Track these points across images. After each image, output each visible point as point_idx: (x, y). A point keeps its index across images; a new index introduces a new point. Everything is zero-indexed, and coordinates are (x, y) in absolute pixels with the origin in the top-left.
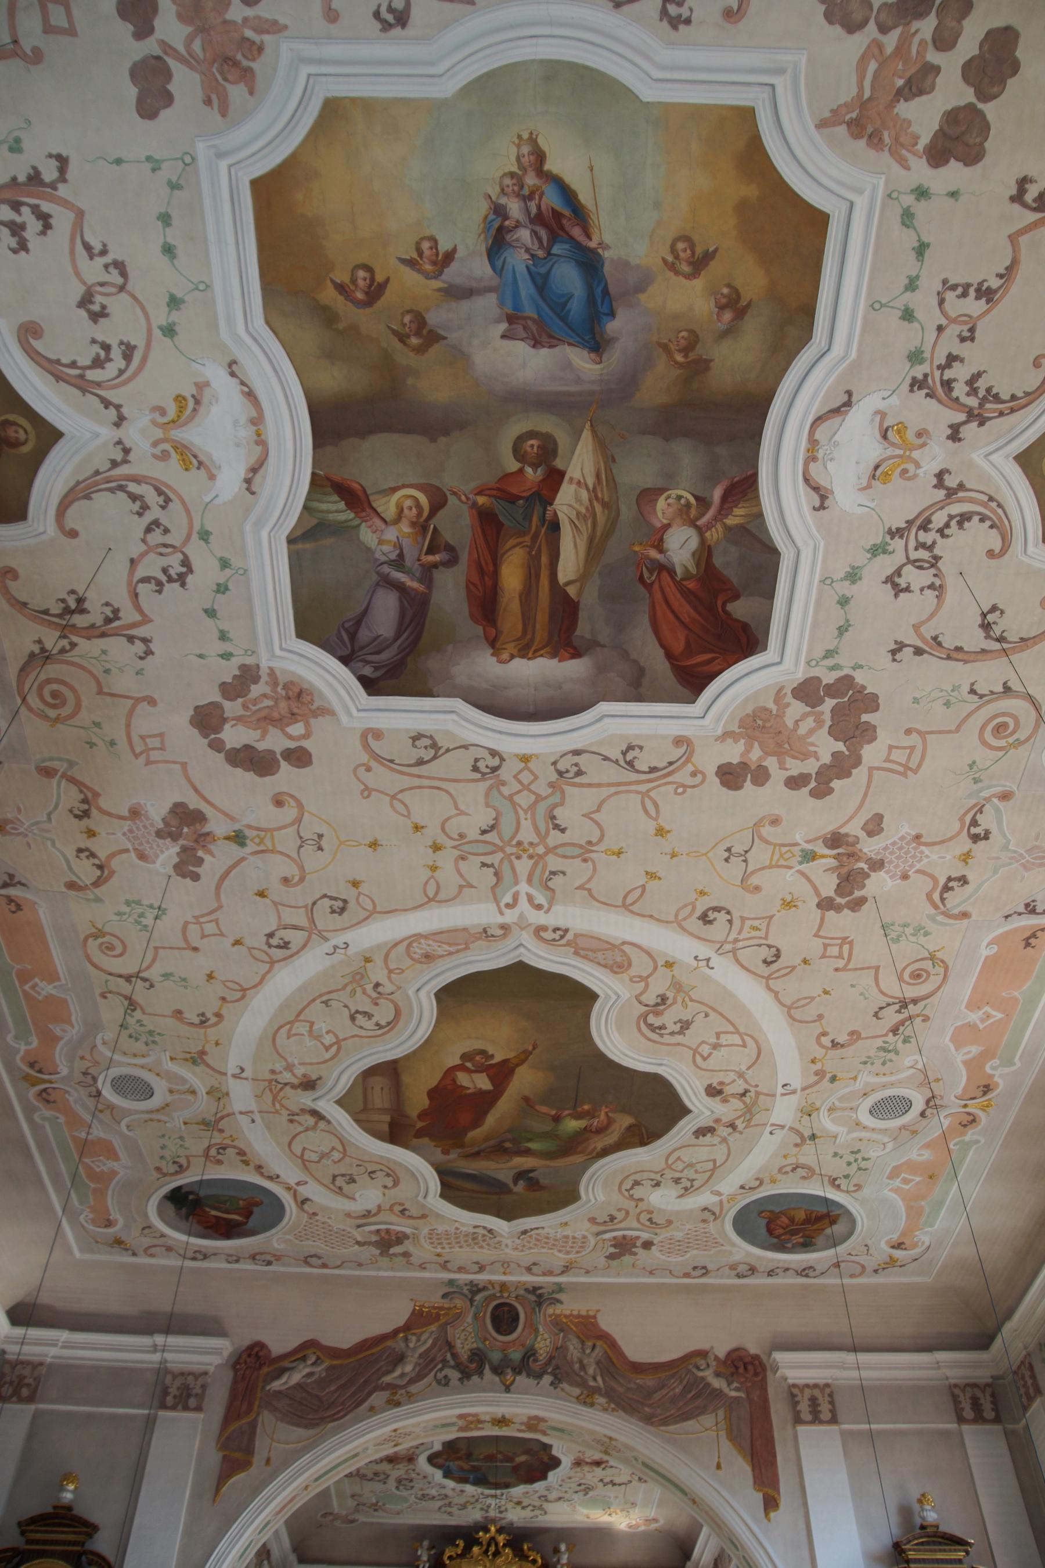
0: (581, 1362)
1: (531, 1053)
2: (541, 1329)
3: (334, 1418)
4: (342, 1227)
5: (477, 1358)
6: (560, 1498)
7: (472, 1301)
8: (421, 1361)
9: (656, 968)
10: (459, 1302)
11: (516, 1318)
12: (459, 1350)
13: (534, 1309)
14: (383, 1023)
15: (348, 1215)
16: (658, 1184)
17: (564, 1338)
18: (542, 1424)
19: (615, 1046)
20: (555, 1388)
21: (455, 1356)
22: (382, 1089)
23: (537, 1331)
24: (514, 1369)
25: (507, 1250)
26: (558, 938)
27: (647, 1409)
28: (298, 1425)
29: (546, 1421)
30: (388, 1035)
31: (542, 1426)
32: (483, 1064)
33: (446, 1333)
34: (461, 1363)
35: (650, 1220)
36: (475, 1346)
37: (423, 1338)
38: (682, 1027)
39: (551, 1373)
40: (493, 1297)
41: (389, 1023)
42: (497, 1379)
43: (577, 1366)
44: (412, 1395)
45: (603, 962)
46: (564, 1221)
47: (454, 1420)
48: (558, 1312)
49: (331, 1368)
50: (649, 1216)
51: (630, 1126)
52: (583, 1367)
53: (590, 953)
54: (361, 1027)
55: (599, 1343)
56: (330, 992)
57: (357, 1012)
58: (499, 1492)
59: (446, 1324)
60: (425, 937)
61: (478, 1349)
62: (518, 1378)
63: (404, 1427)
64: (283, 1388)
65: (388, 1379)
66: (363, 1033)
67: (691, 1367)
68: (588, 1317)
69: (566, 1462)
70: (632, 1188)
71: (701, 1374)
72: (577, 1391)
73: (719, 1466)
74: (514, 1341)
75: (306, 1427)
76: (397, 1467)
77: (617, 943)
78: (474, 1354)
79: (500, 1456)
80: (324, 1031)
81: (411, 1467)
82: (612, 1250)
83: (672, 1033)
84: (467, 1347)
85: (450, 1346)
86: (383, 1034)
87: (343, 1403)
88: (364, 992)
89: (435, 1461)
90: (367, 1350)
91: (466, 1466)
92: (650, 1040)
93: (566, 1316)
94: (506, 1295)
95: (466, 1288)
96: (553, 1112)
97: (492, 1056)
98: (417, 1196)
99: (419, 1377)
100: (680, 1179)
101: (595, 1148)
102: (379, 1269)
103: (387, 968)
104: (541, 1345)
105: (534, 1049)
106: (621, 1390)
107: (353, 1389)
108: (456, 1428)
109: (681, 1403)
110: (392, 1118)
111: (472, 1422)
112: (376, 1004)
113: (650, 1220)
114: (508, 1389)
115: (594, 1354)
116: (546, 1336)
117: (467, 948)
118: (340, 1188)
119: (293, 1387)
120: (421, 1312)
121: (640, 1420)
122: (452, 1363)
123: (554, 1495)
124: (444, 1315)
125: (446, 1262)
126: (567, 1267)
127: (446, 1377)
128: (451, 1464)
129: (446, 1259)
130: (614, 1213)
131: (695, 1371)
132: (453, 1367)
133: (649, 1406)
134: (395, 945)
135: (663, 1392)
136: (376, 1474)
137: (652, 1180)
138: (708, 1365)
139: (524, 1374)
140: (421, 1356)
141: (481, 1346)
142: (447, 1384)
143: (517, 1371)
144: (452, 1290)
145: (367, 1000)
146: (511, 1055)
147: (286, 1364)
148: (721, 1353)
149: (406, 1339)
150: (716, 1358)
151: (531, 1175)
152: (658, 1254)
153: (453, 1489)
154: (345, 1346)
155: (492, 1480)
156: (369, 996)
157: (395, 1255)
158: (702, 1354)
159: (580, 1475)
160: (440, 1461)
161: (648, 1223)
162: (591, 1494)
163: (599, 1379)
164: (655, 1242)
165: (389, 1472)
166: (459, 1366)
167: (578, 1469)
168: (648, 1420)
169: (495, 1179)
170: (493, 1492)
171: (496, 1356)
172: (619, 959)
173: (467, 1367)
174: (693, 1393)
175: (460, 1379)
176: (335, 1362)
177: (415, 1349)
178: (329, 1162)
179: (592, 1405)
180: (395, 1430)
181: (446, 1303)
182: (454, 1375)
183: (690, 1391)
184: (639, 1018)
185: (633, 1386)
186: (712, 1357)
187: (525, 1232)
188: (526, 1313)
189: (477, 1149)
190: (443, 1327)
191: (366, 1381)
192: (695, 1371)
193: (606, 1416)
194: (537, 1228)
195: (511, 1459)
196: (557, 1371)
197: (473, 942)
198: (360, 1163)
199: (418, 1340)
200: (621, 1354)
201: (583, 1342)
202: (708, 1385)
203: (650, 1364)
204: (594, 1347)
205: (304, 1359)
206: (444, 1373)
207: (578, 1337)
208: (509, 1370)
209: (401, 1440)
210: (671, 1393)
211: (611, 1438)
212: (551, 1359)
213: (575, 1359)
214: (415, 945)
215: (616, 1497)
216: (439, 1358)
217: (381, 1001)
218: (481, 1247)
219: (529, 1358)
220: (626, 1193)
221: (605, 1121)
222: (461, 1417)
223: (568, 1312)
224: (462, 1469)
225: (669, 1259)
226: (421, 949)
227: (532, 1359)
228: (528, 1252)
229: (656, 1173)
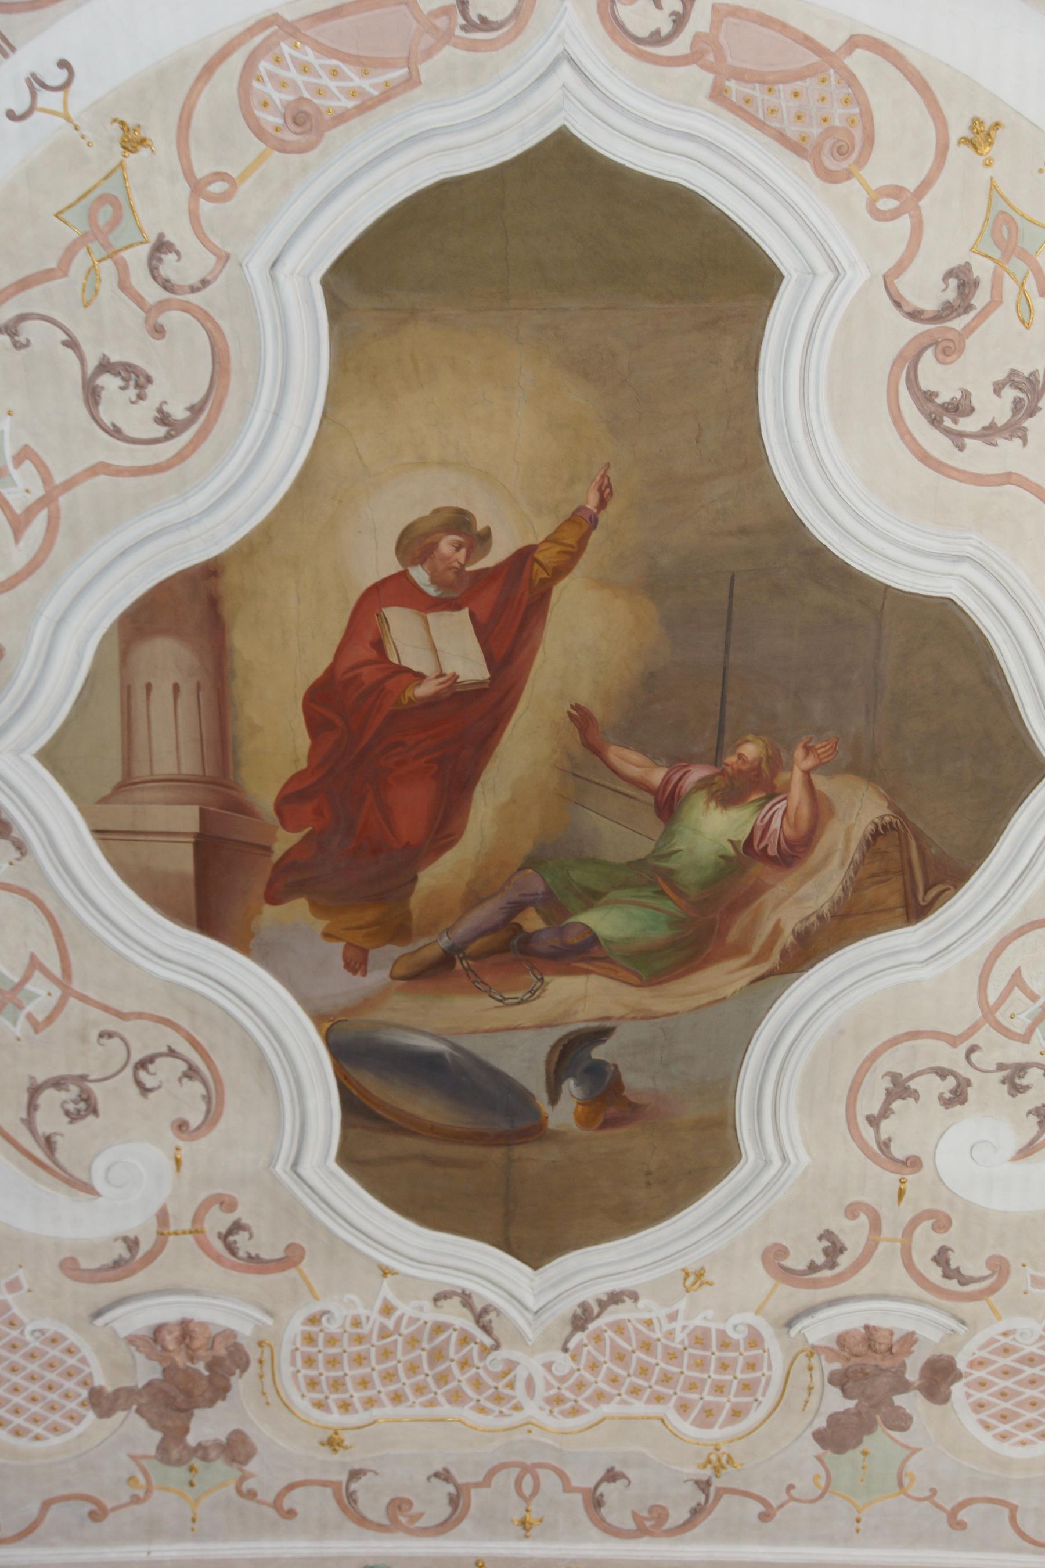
1: (594, 522)
4: (52, 1326)
9: (942, 150)
14: (179, 413)
15: (70, 1267)
16: (958, 1096)
19: (833, 487)
22: (176, 688)
25: (533, 1410)
26: (666, 28)
30: (194, 462)
32: (460, 571)
35: (941, 1258)
38: (1017, 404)
41: (195, 410)
45: (793, 131)
46: (691, 1261)
50: (939, 1240)
51: (876, 835)
53: (757, 92)
54: (116, 432)
56: (24, 284)
57: (105, 367)
60: (292, 30)
66: (124, 455)
70: (886, 1112)
77: (833, 42)
80: (9, 452)
82: (836, 1402)
83: (989, 433)
86: (180, 457)
88: (124, 285)
92: (925, 458)
96: (657, 776)
97: (485, 537)
98: (273, 1160)
100: (1021, 1069)
101: (777, 931)
102: (153, 1531)
103: (188, 173)
105: (602, 504)
110: (204, 816)
112: (158, 331)
113: (941, 1258)
117: (412, 81)
118: (49, 1143)
125: (355, 1474)
126: (704, 1485)
129: (354, 1458)
130: (840, 1226)
134: (209, 70)
137: (942, 1073)
145: (134, 316)
146: (538, 531)
151: (598, 1053)
152: (970, 1421)
156: (138, 299)
157: (202, 1451)
161: (935, 1274)
164: (961, 1365)
169: (496, 1074)
172: (838, 115)
178: (21, 1028)
184: (900, 357)
187: (581, 1319)
189: (444, 942)
194: (615, 1298)
197: (429, 53)
198: (111, 1023)
214: (264, 66)
217: (173, 319)
218: (457, 1397)
220: (868, 1133)
221: (805, 811)
225: (1008, 1450)
226: (283, 84)
228: (593, 1413)
229: (954, 1041)
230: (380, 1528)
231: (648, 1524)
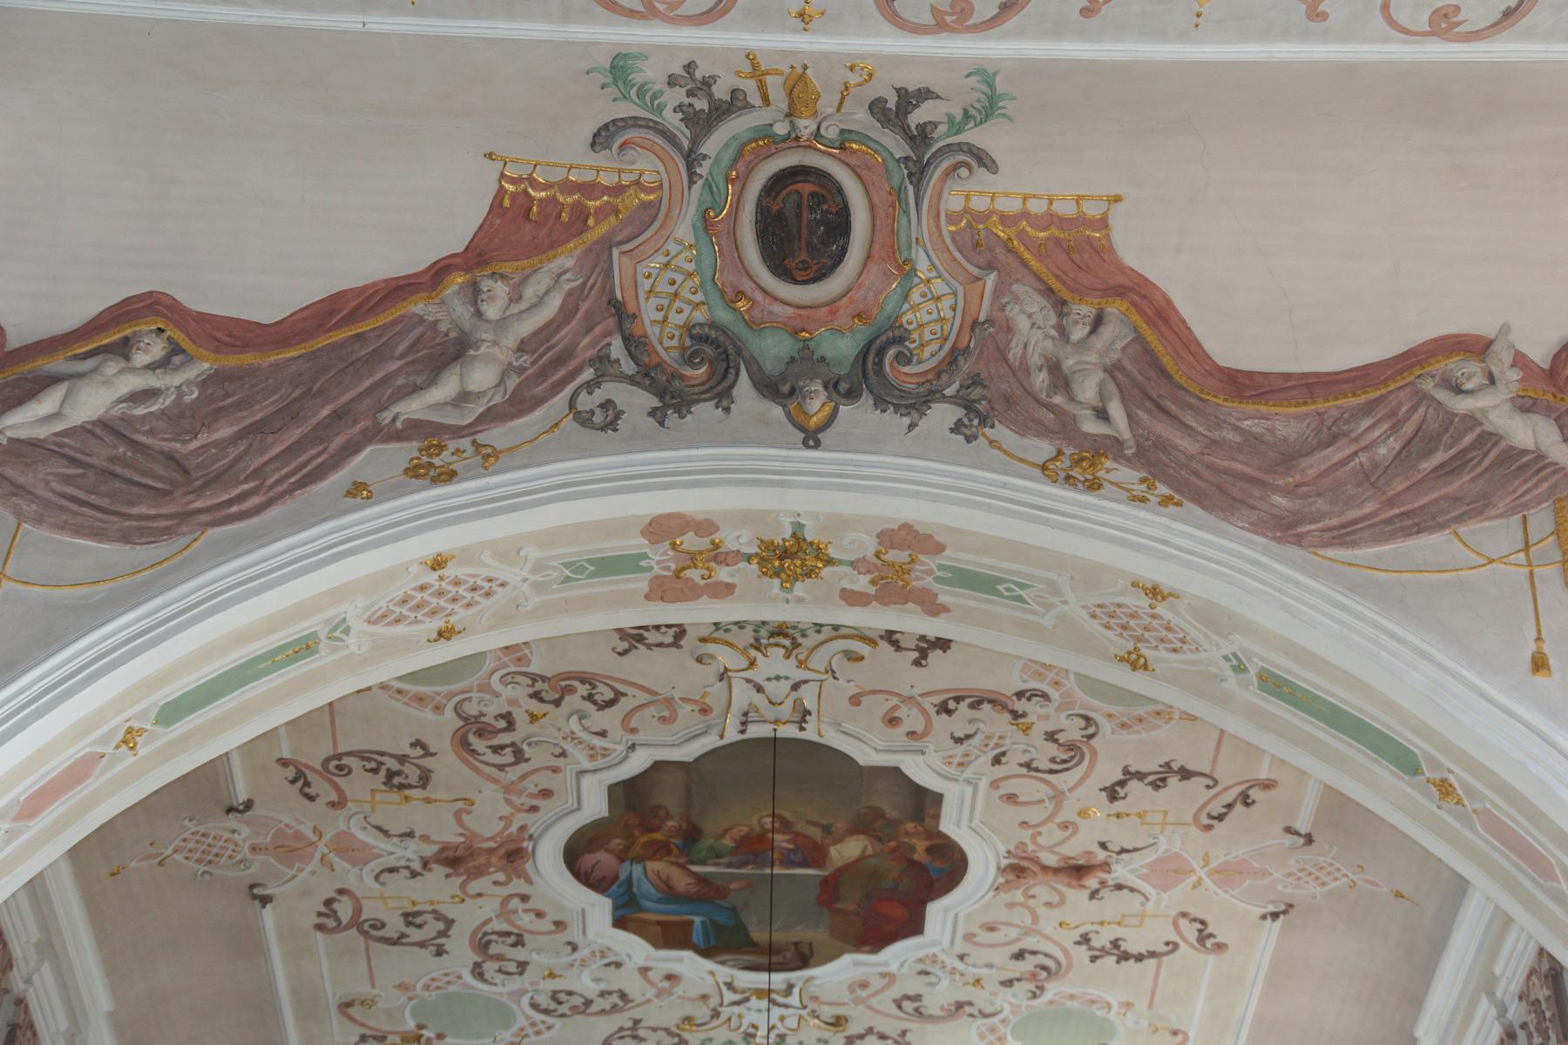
0: (1054, 368)
2: (922, 265)
3: (222, 516)
5: (709, 350)
6: (960, 1006)
7: (692, 159)
8: (526, 359)
10: (646, 165)
11: (840, 226)
12: (653, 332)
13: (899, 193)
17: (997, 293)
18: (929, 562)
20: (968, 439)
21: (635, 344)
23: (906, 270)
24: (832, 386)
27: (1279, 500)
28: (99, 534)
29: (940, 548)
31: (924, 577)
33: (608, 273)
34: (660, 365)
36: (700, 316)
37: (531, 292)
39: (954, 400)
40: (766, 141)
42: (777, 411)
43: (1041, 380)
44: (496, 454)
47: (637, 543)
48: (979, 204)
49: (218, 378)
52: (1061, 380)
55: (1114, 309)
58: (779, 979)
59: (607, 244)
61: (713, 325)
62: (844, 409)
63: (468, 554)
64: (42, 432)
65: (413, 408)
67: (1428, 385)
68: (1081, 221)
69: (983, 863)
71: (1463, 405)
72: (1042, 449)
73: (1539, 664)
74: (832, 304)
75: (126, 538)
76: (474, 887)
78: (702, 339)
79: (780, 839)
81: (518, 886)
84: (677, 320)
85: (621, 314)
87: (258, 473)
89: (588, 860)
90: (340, 325)
91: (682, 882)
93: (1005, 219)
94: (806, 126)
95: (678, 96)
99: (519, 404)
104: (923, 316)
106: (1184, 443)
107: (294, 435)
108: (641, 584)
109: (1399, 485)
111: (693, 558)
114: (812, 439)
115: (1099, 342)
116: (939, 287)
119: (84, 430)
120: (523, 205)
121: (1255, 528)
122: (628, 367)
123: (939, 996)
124: (601, 214)
127: (607, 405)
128: (637, 870)
131: (1442, 395)
132: (631, 380)
133: (1288, 492)
135: (1336, 454)
136: (410, 918)
138: (1492, 379)
139: (867, 399)
140: (522, 347)
141: (724, 316)
142: (611, 425)
143: (844, 389)
144: (625, 110)
147: (56, 364)
148: (1540, 352)
149: (474, 294)
150: (1520, 360)
153: (644, 971)
154: (267, 316)
155: (759, 935)
158: (1476, 347)
159: (1022, 917)
160: (602, 859)
162: (1053, 989)
163: (1116, 410)
165: (450, 911)
166: (650, 375)
167: (1018, 896)
168: (1285, 529)
170: (759, 979)
171: (773, 349)
173: (681, 377)
174: (1440, 457)
175: (653, 413)
176: (231, 361)
177: (503, 323)
179: (1094, 486)
180: (438, 564)
181: (605, 169)
182: (636, 402)
183: (1428, 453)
185: (1230, 436)
186: (1508, 358)
188: (872, 207)
190: (599, 257)
191: (338, 415)
192: (1442, 395)
193: (1143, 514)
195: (813, 854)
196: (977, 392)
199: (515, 298)
200: (1189, 344)
201: (1061, 306)
202: (1490, 439)
203: (1288, 376)
204: (1098, 322)
205: (123, 349)
206: (600, 395)
207: (1049, 292)
208: (817, 386)
209: (460, 616)
210: (1363, 457)
211: (1154, 592)
212: (955, 356)
213: (1035, 359)
215: (1128, 1005)
216: (585, 351)
219: (881, 352)
222: (660, 529)
223: (1012, 206)
224: (669, 893)
227: (891, 353)
230: (632, 14)
231: (948, 19)
